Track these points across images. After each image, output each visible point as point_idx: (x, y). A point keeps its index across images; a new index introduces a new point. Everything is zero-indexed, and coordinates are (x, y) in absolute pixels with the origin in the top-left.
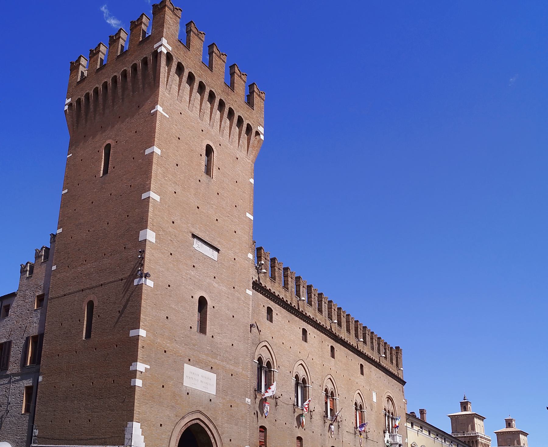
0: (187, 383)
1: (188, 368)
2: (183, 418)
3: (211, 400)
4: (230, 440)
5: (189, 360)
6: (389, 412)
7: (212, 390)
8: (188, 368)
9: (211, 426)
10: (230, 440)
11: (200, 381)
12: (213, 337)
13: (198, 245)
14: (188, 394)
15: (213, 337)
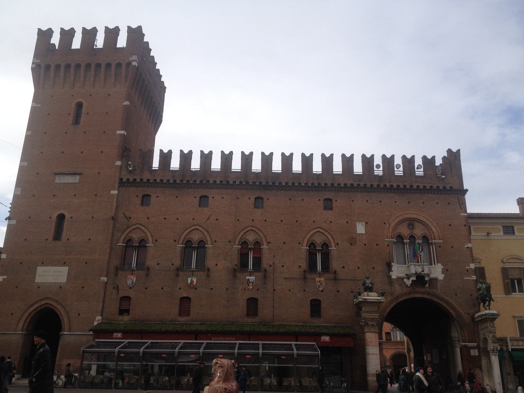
0: (38, 279)
1: (40, 269)
2: (32, 305)
3: (61, 287)
4: (79, 314)
5: (43, 263)
6: (412, 238)
7: (63, 279)
8: (40, 269)
9: (59, 307)
10: (79, 314)
11: (52, 275)
12: (68, 240)
13: (59, 180)
14: (39, 287)
15: (68, 240)
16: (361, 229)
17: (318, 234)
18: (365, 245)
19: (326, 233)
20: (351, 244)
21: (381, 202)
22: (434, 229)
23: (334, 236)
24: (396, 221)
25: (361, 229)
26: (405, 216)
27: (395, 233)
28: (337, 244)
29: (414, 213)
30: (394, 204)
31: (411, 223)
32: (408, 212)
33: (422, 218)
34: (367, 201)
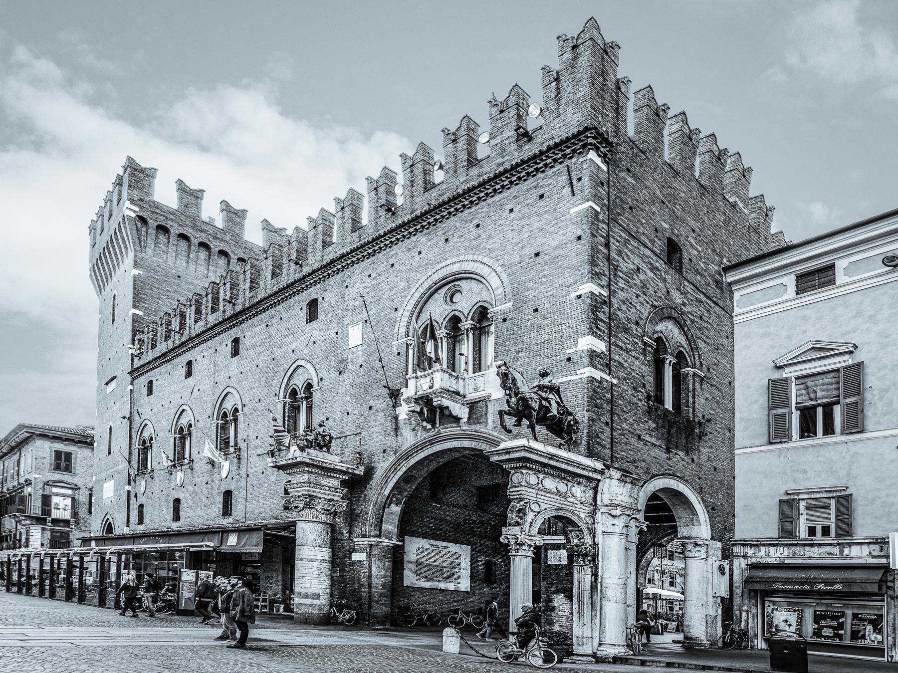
16: (355, 335)
17: (300, 370)
18: (361, 366)
19: (308, 366)
20: (340, 373)
21: (392, 265)
22: (494, 281)
23: (318, 367)
24: (417, 295)
25: (355, 335)
26: (436, 277)
27: (420, 323)
28: (322, 379)
29: (455, 260)
30: (417, 258)
31: (450, 284)
32: (444, 264)
33: (469, 267)
34: (370, 276)
